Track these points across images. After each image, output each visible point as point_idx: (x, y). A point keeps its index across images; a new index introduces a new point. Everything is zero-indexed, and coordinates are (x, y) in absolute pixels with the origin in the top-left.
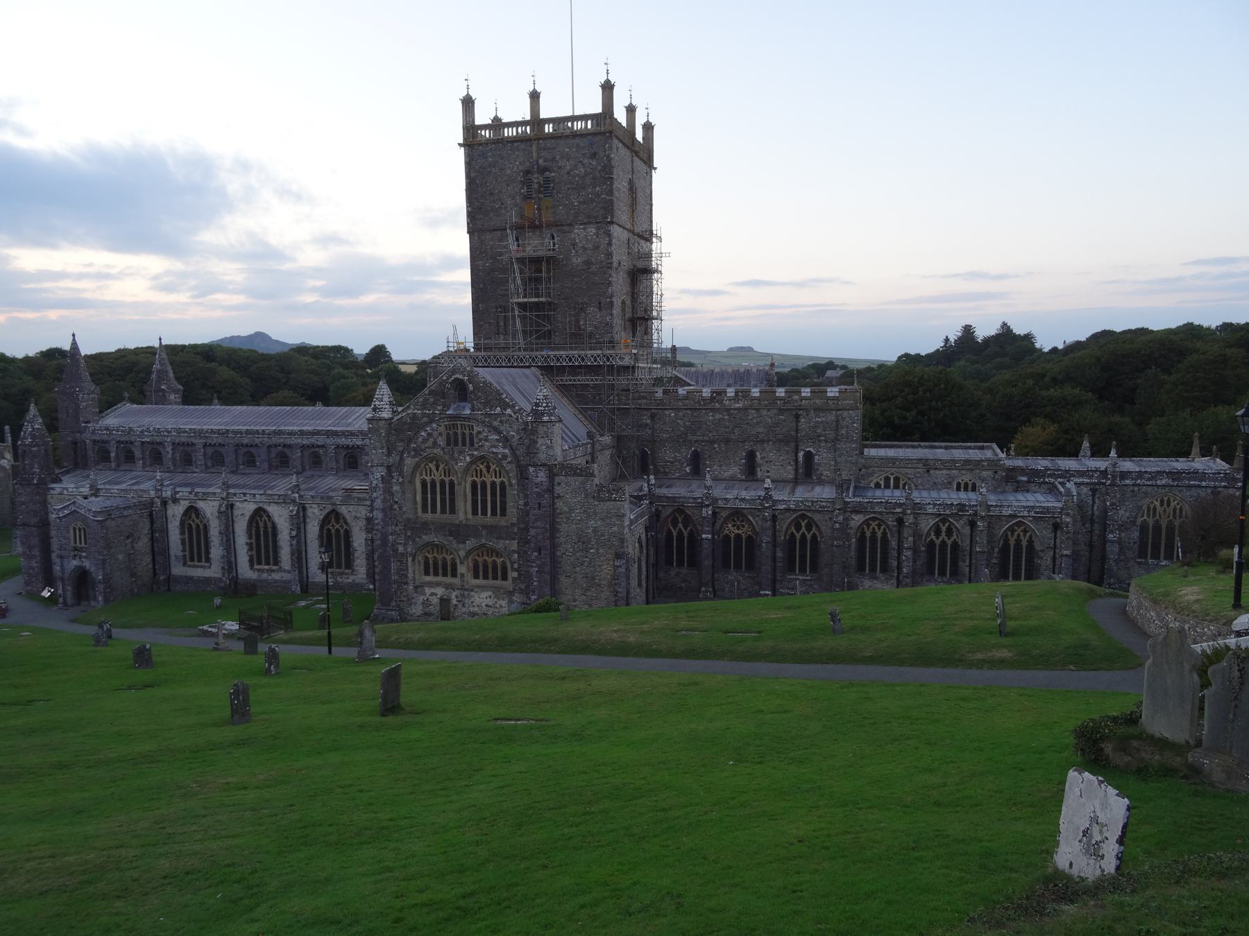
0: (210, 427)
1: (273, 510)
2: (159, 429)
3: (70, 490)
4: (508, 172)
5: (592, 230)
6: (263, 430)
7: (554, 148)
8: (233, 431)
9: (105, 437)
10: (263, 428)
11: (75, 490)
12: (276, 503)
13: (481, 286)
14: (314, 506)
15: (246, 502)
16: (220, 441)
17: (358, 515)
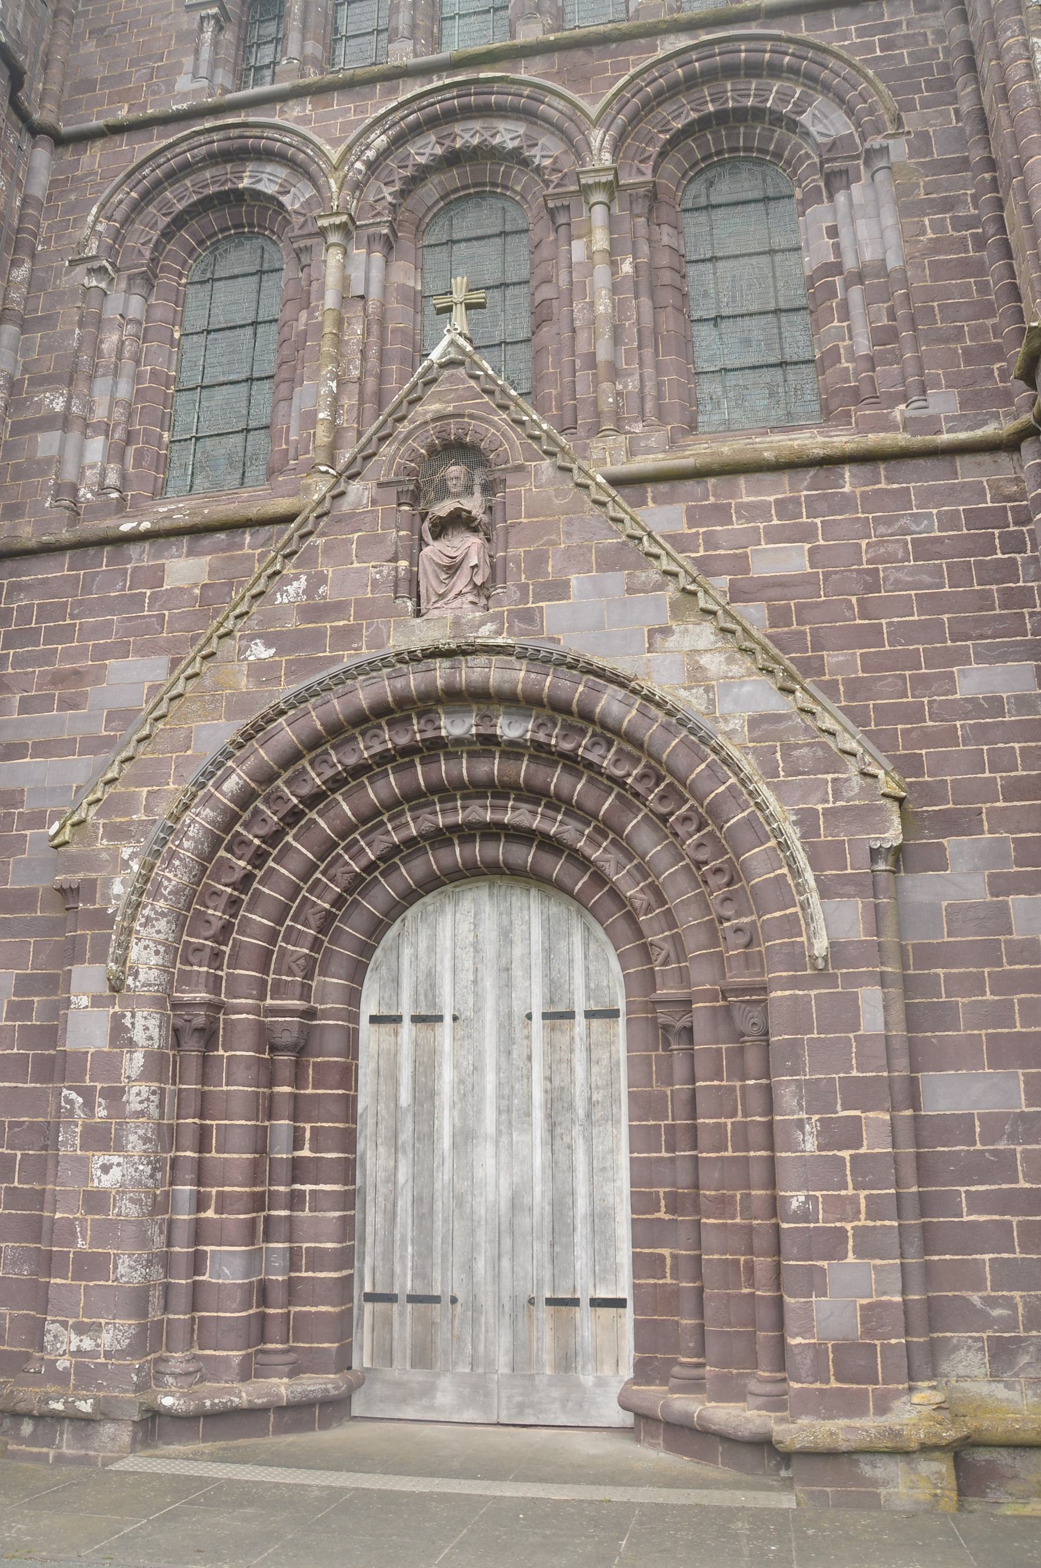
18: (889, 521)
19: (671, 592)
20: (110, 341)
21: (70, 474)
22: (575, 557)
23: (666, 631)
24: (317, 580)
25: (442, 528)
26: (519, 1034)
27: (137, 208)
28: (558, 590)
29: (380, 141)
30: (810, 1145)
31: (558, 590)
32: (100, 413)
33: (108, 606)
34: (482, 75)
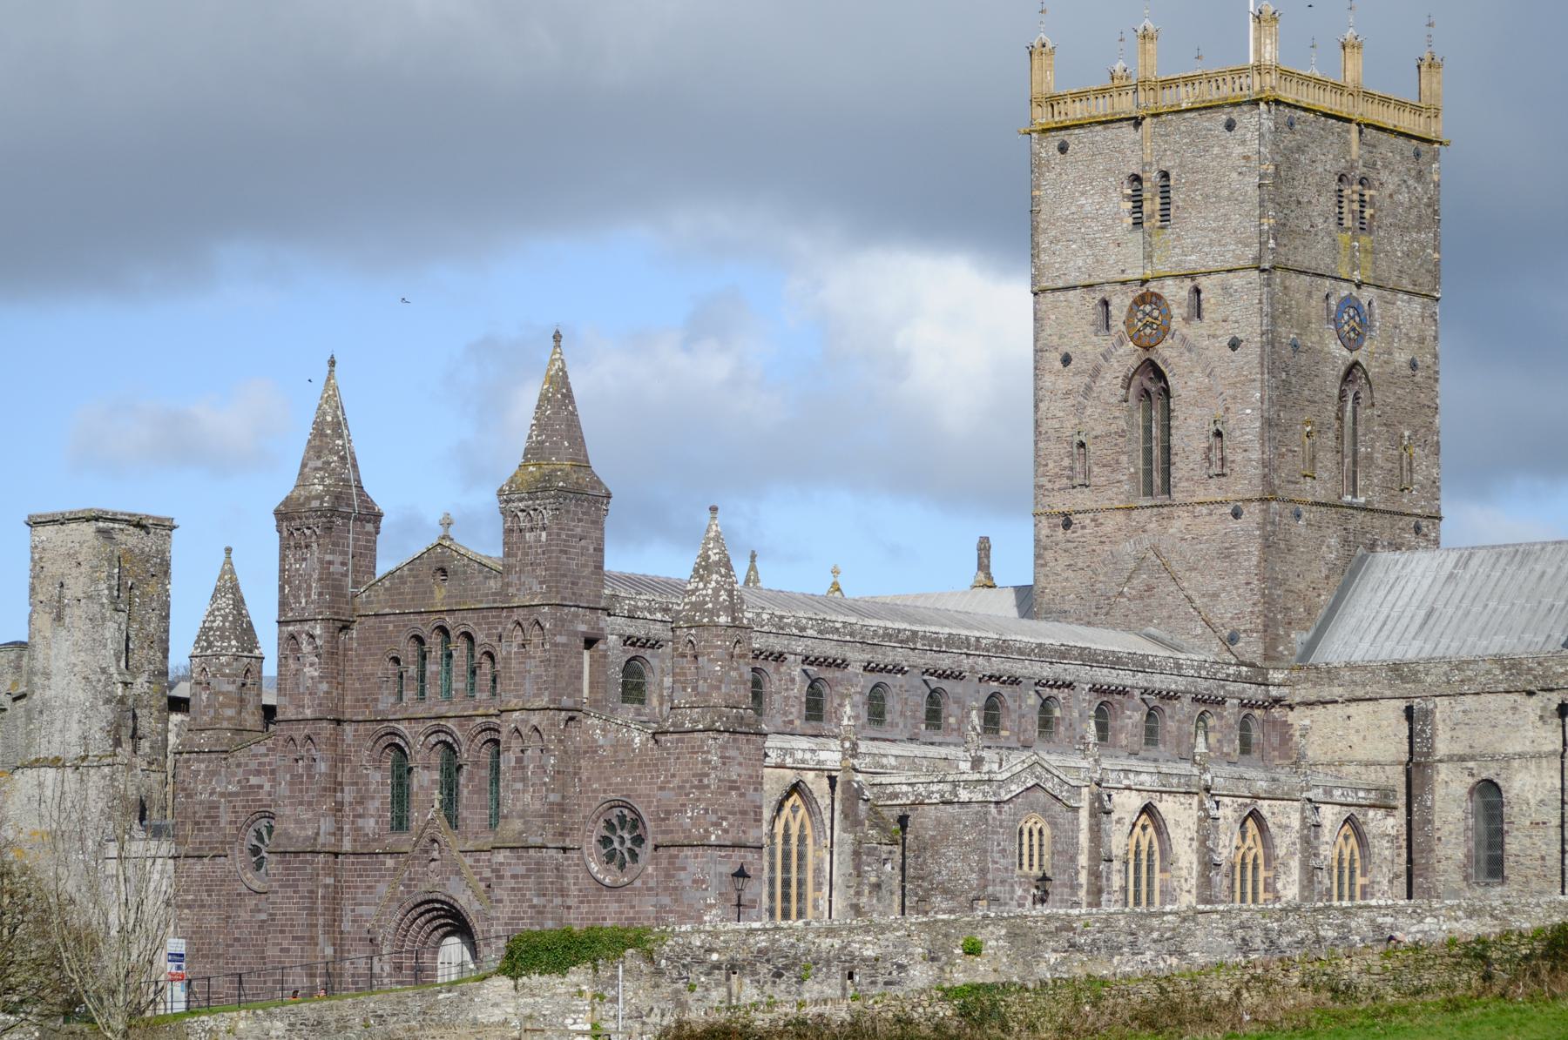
0: (882, 623)
1: (1166, 806)
2: (781, 617)
3: (799, 755)
4: (1320, 170)
5: (1417, 305)
6: (978, 639)
7: (1375, 146)
8: (924, 637)
9: (658, 631)
10: (978, 634)
11: (808, 756)
12: (1170, 792)
13: (1284, 376)
14: (1227, 800)
15: (1127, 792)
16: (898, 659)
17: (1285, 821)
20: (372, 787)
28: (448, 879)
31: (448, 879)
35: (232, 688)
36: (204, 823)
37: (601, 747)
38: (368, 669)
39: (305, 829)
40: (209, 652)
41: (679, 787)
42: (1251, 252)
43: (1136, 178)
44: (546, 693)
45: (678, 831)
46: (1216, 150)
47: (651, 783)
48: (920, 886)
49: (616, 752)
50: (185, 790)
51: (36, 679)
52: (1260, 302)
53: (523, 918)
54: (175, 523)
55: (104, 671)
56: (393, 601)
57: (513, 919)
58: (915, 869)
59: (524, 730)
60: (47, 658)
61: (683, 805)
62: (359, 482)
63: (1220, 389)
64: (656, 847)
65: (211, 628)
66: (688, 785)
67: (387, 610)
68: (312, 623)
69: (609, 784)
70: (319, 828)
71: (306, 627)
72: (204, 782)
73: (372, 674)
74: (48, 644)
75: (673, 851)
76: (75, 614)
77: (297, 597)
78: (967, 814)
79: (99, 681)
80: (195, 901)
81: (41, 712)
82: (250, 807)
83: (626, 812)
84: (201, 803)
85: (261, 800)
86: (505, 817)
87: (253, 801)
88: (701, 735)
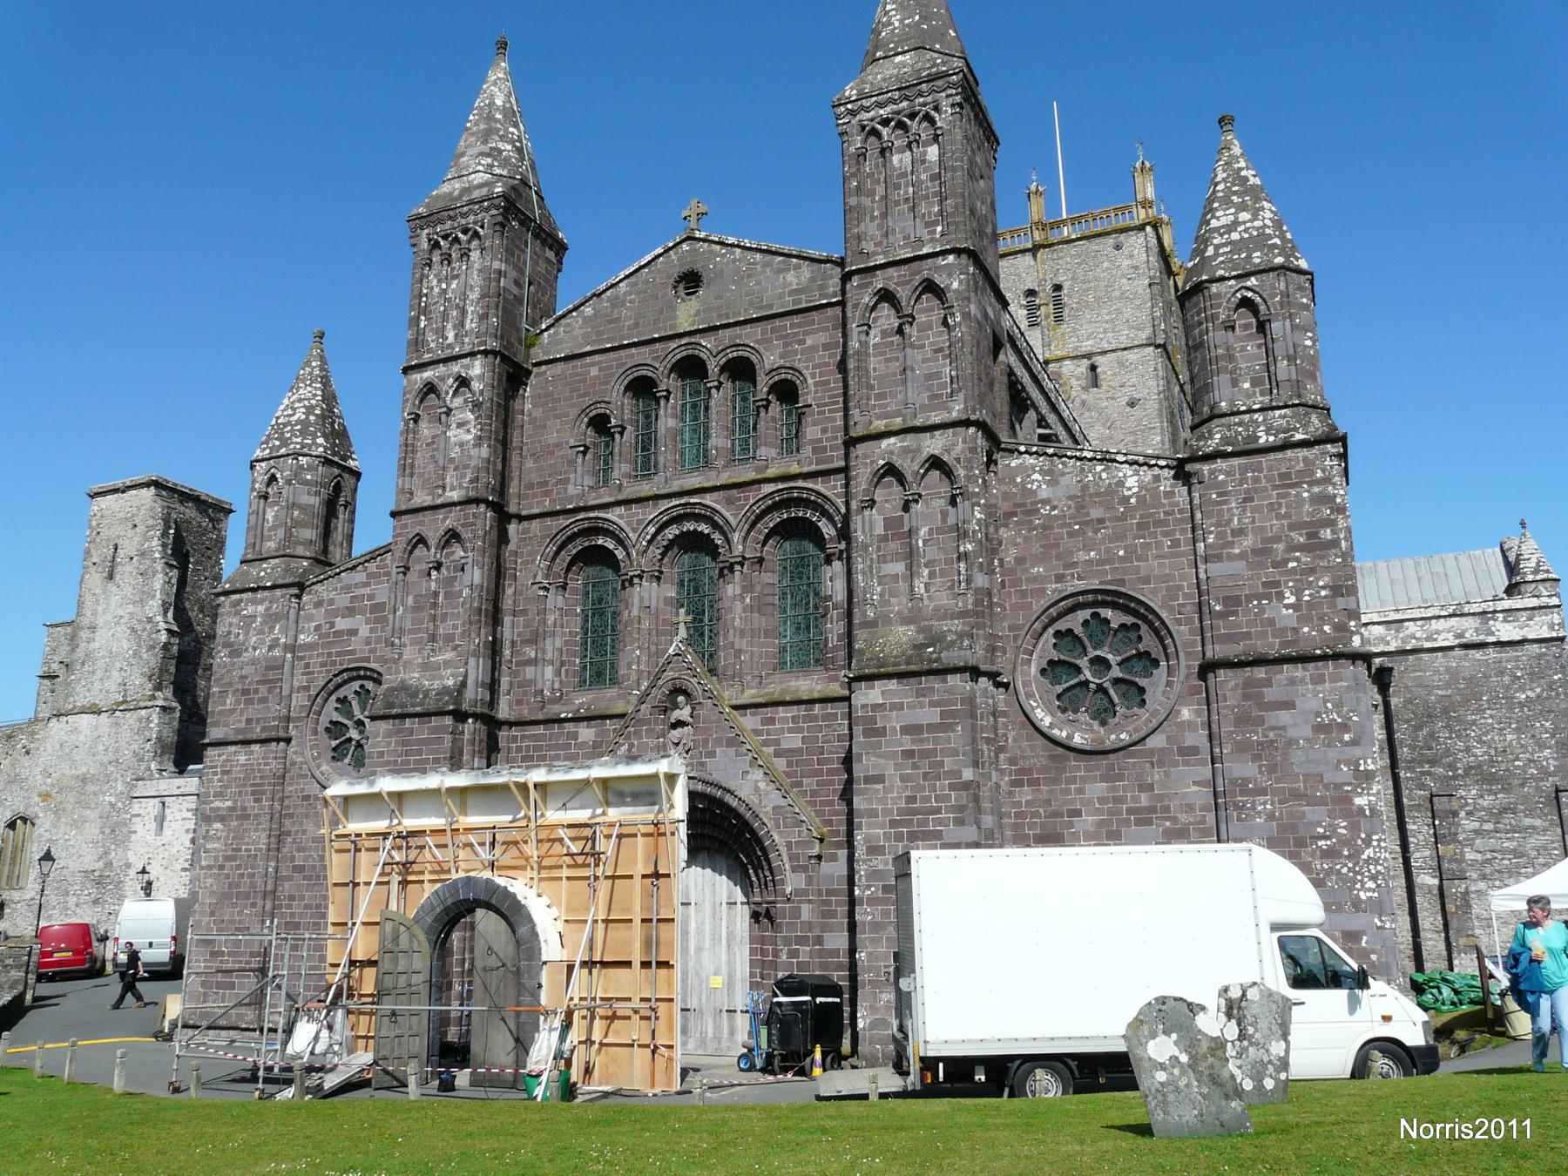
18: (830, 726)
19: (749, 757)
20: (551, 619)
21: (539, 687)
22: (718, 742)
23: (747, 772)
24: (631, 746)
25: (674, 726)
26: (718, 910)
27: (557, 553)
28: (712, 754)
29: (652, 530)
30: (784, 957)
31: (712, 754)
32: (549, 656)
33: (558, 747)
34: (692, 501)
35: (314, 501)
36: (256, 691)
37: (1045, 502)
38: (552, 437)
39: (441, 678)
40: (283, 451)
41: (1255, 551)
42: (1143, 336)
43: (1031, 293)
44: (961, 396)
45: (1262, 635)
46: (1106, 265)
47: (1172, 555)
48: (1429, 773)
49: (1080, 507)
50: (231, 644)
51: (82, 633)
52: (1156, 369)
53: (938, 811)
54: (233, 508)
55: (150, 620)
56: (599, 333)
57: (914, 812)
58: (1412, 748)
59: (910, 467)
60: (95, 613)
61: (1277, 584)
62: (539, 188)
63: (1121, 437)
64: (1207, 669)
65: (285, 425)
66: (1281, 546)
67: (588, 348)
68: (466, 361)
69: (1074, 565)
70: (466, 677)
71: (456, 368)
72: (261, 632)
73: (557, 445)
74: (97, 600)
75: (1260, 673)
76: (125, 572)
77: (441, 332)
78: (1517, 659)
79: (145, 629)
80: (232, 809)
81: (83, 664)
82: (334, 663)
83: (1107, 613)
84: (253, 662)
85: (352, 652)
86: (871, 624)
87: (339, 654)
88: (1302, 453)
